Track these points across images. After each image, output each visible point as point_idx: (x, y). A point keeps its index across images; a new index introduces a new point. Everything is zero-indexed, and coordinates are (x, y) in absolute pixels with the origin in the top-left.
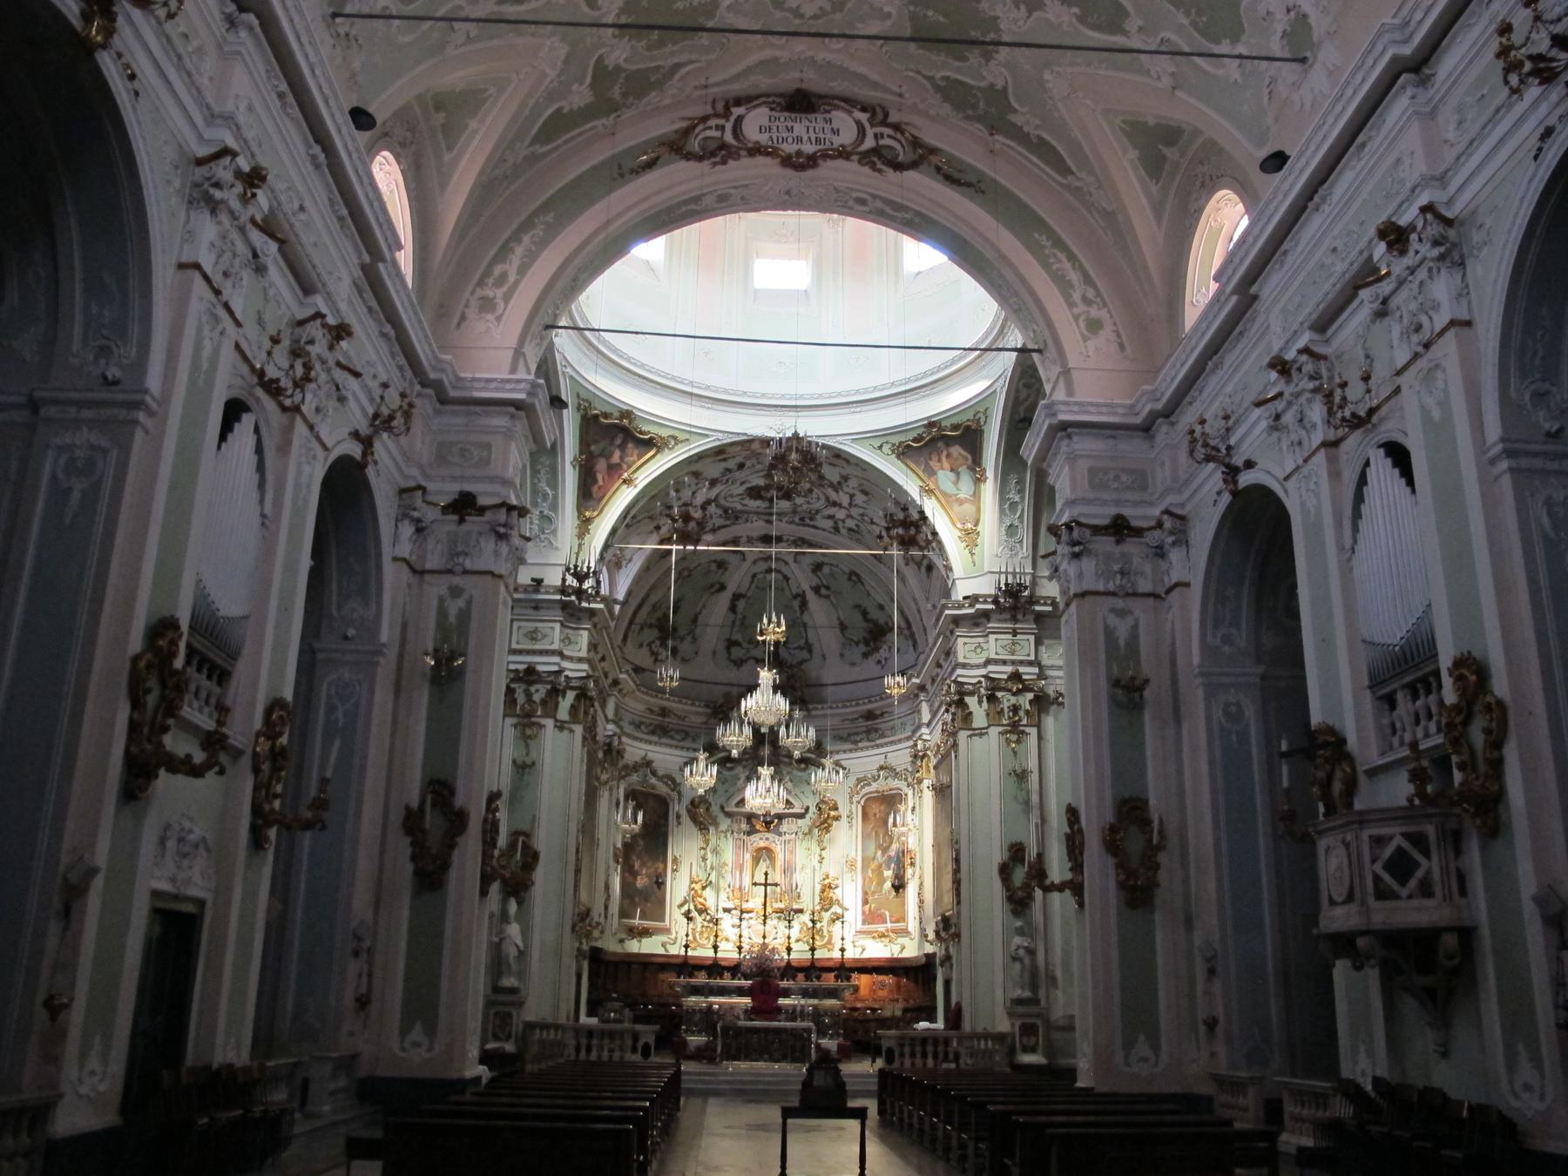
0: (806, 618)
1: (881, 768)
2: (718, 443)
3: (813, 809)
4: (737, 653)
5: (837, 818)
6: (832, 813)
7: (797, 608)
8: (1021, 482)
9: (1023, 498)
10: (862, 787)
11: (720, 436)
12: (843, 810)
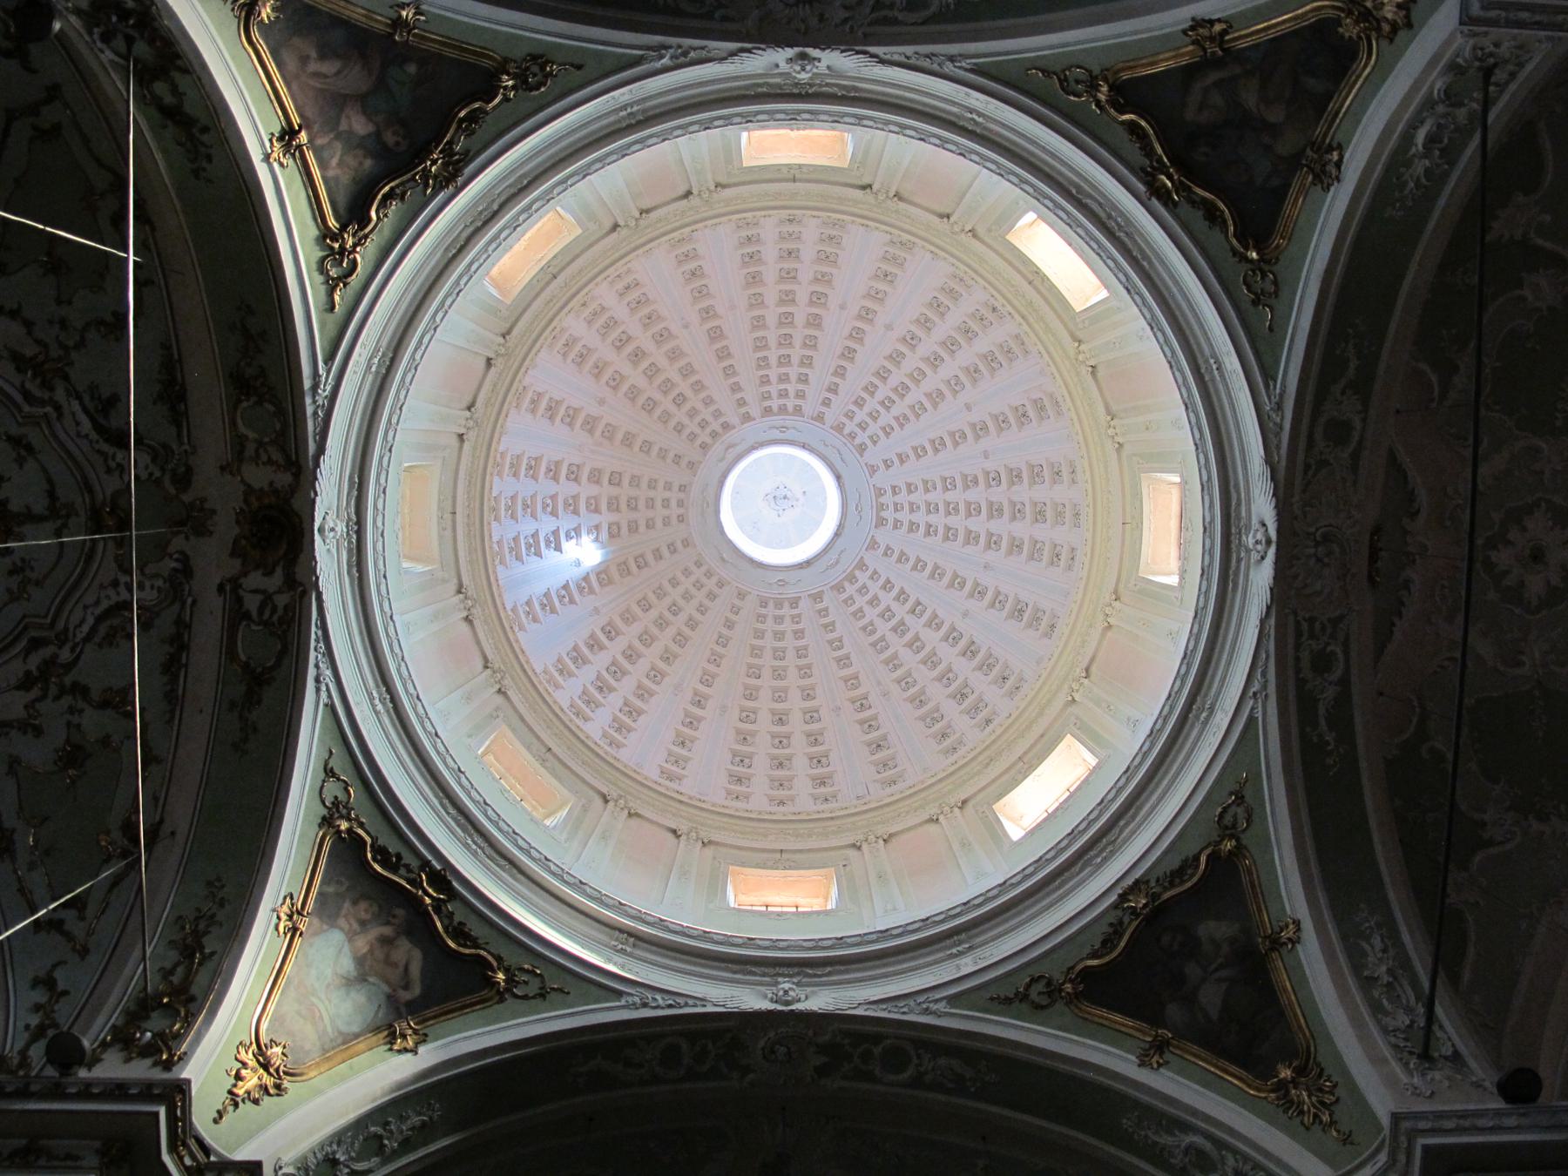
2: (307, 384)
8: (425, 1132)
9: (396, 1154)
11: (325, 391)
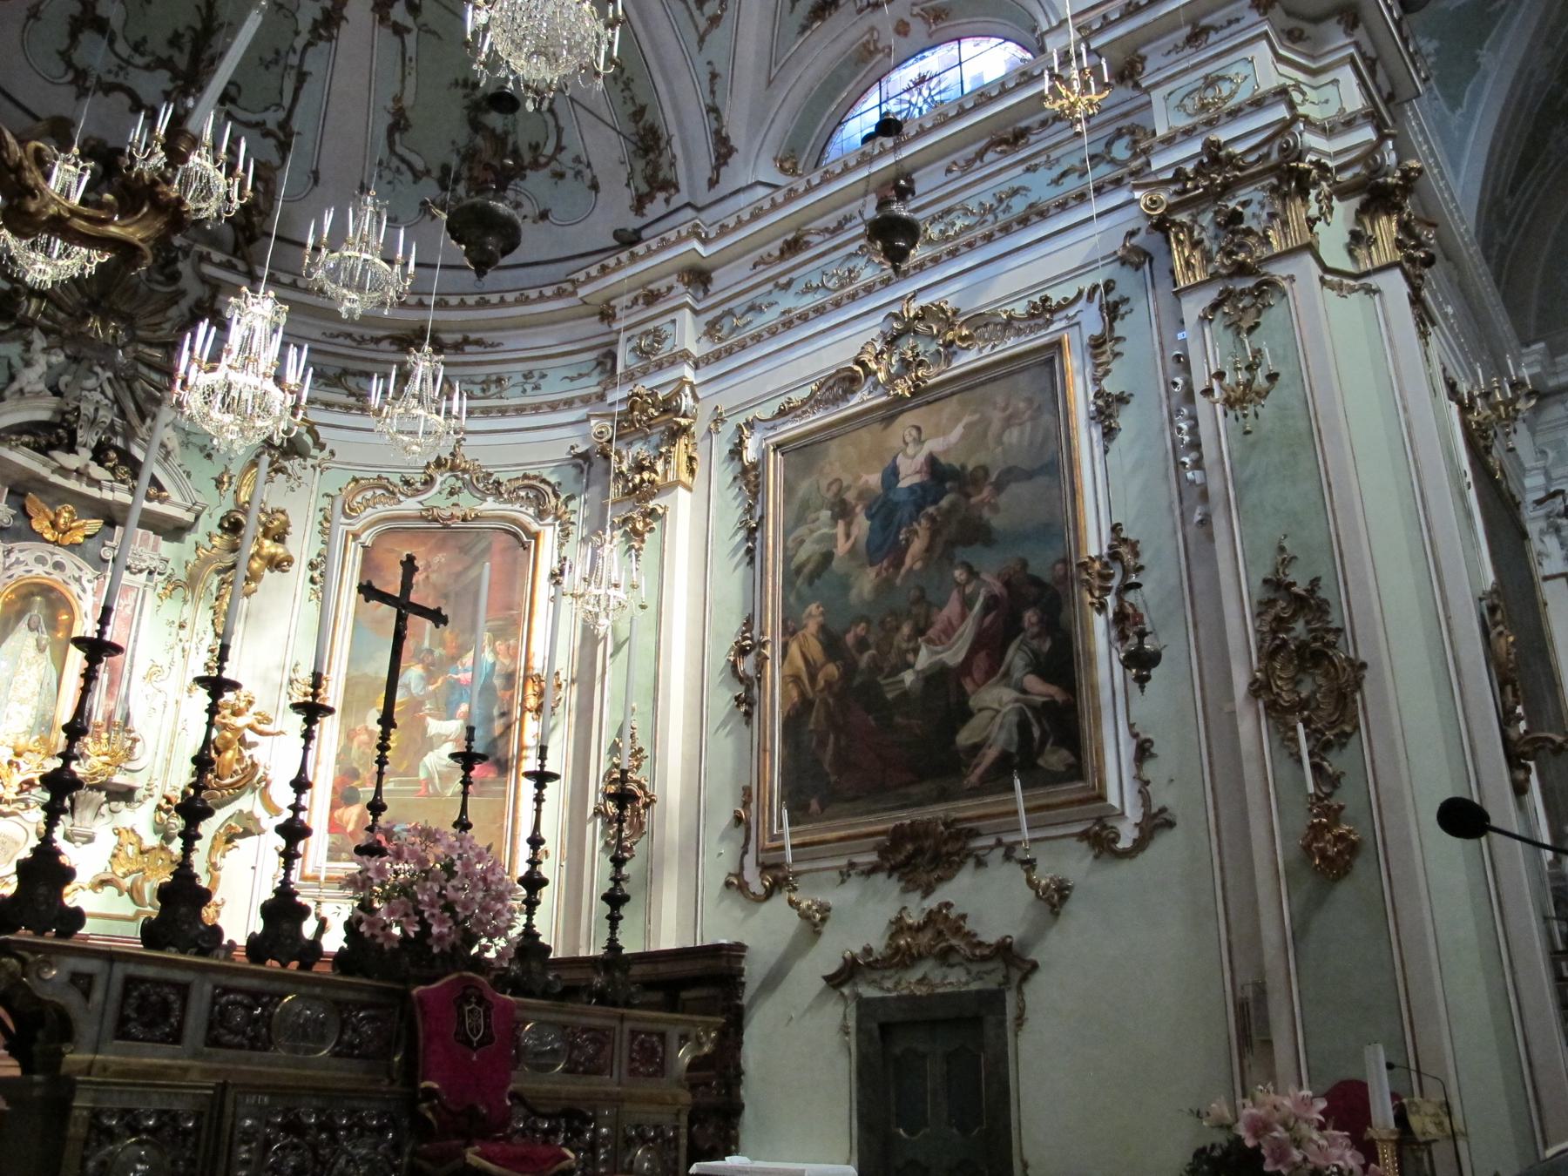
0: (314, 63)
1: (439, 463)
3: (209, 523)
4: (94, 54)
5: (276, 564)
6: (269, 547)
7: (305, 24)
10: (367, 504)
12: (302, 545)
